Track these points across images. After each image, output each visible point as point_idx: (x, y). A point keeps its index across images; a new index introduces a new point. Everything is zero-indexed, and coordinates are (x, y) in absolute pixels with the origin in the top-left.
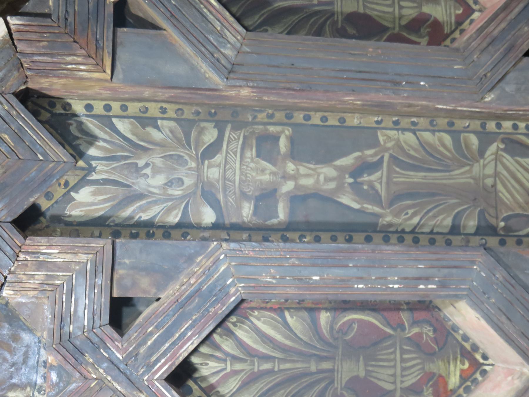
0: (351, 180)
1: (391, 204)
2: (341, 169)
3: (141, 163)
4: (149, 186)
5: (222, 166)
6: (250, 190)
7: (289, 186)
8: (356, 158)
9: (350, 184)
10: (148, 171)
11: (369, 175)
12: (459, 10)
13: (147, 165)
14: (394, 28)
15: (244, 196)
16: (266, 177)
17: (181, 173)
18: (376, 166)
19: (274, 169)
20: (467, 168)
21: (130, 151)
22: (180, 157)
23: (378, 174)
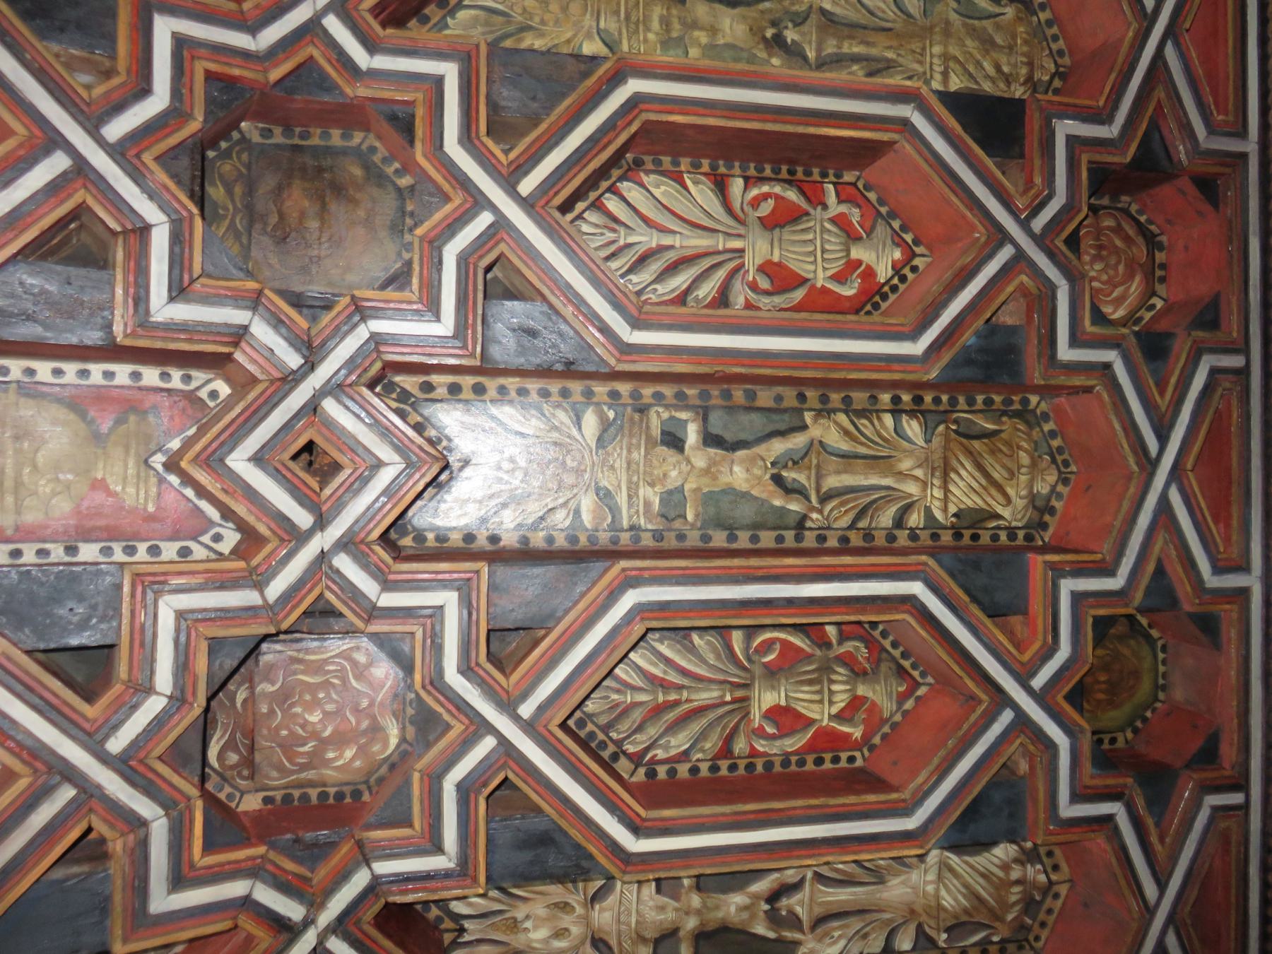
0: (767, 907)
1: (813, 928)
2: (756, 897)
3: (520, 915)
4: (532, 941)
5: (616, 909)
6: (650, 934)
7: (691, 923)
8: (773, 881)
9: (766, 912)
10: (528, 924)
11: (789, 898)
12: (901, 685)
13: (528, 917)
14: (822, 720)
15: (642, 939)
16: (670, 915)
17: (566, 921)
18: (796, 886)
19: (676, 904)
20: (903, 878)
21: (510, 905)
22: (566, 904)
23: (798, 896)
